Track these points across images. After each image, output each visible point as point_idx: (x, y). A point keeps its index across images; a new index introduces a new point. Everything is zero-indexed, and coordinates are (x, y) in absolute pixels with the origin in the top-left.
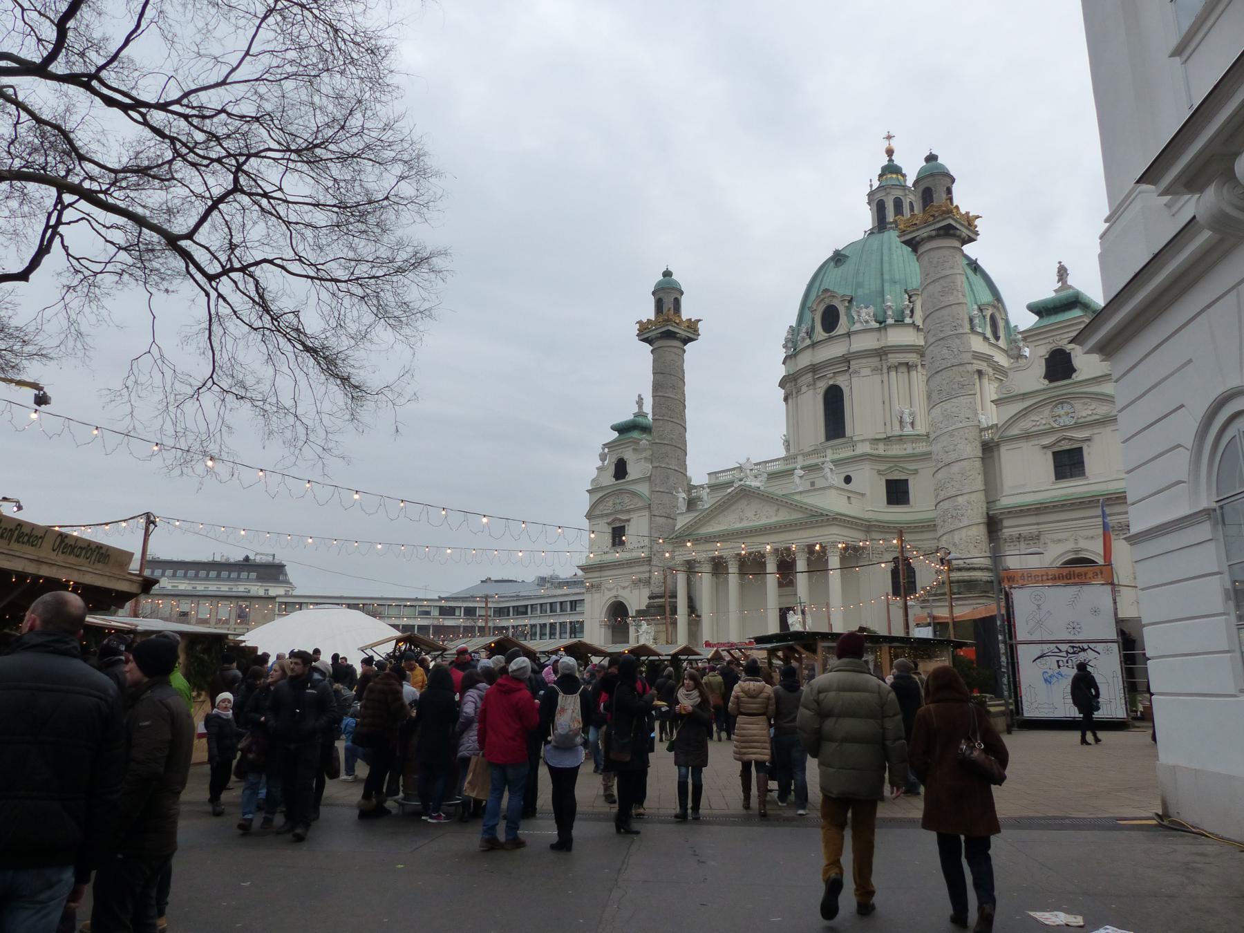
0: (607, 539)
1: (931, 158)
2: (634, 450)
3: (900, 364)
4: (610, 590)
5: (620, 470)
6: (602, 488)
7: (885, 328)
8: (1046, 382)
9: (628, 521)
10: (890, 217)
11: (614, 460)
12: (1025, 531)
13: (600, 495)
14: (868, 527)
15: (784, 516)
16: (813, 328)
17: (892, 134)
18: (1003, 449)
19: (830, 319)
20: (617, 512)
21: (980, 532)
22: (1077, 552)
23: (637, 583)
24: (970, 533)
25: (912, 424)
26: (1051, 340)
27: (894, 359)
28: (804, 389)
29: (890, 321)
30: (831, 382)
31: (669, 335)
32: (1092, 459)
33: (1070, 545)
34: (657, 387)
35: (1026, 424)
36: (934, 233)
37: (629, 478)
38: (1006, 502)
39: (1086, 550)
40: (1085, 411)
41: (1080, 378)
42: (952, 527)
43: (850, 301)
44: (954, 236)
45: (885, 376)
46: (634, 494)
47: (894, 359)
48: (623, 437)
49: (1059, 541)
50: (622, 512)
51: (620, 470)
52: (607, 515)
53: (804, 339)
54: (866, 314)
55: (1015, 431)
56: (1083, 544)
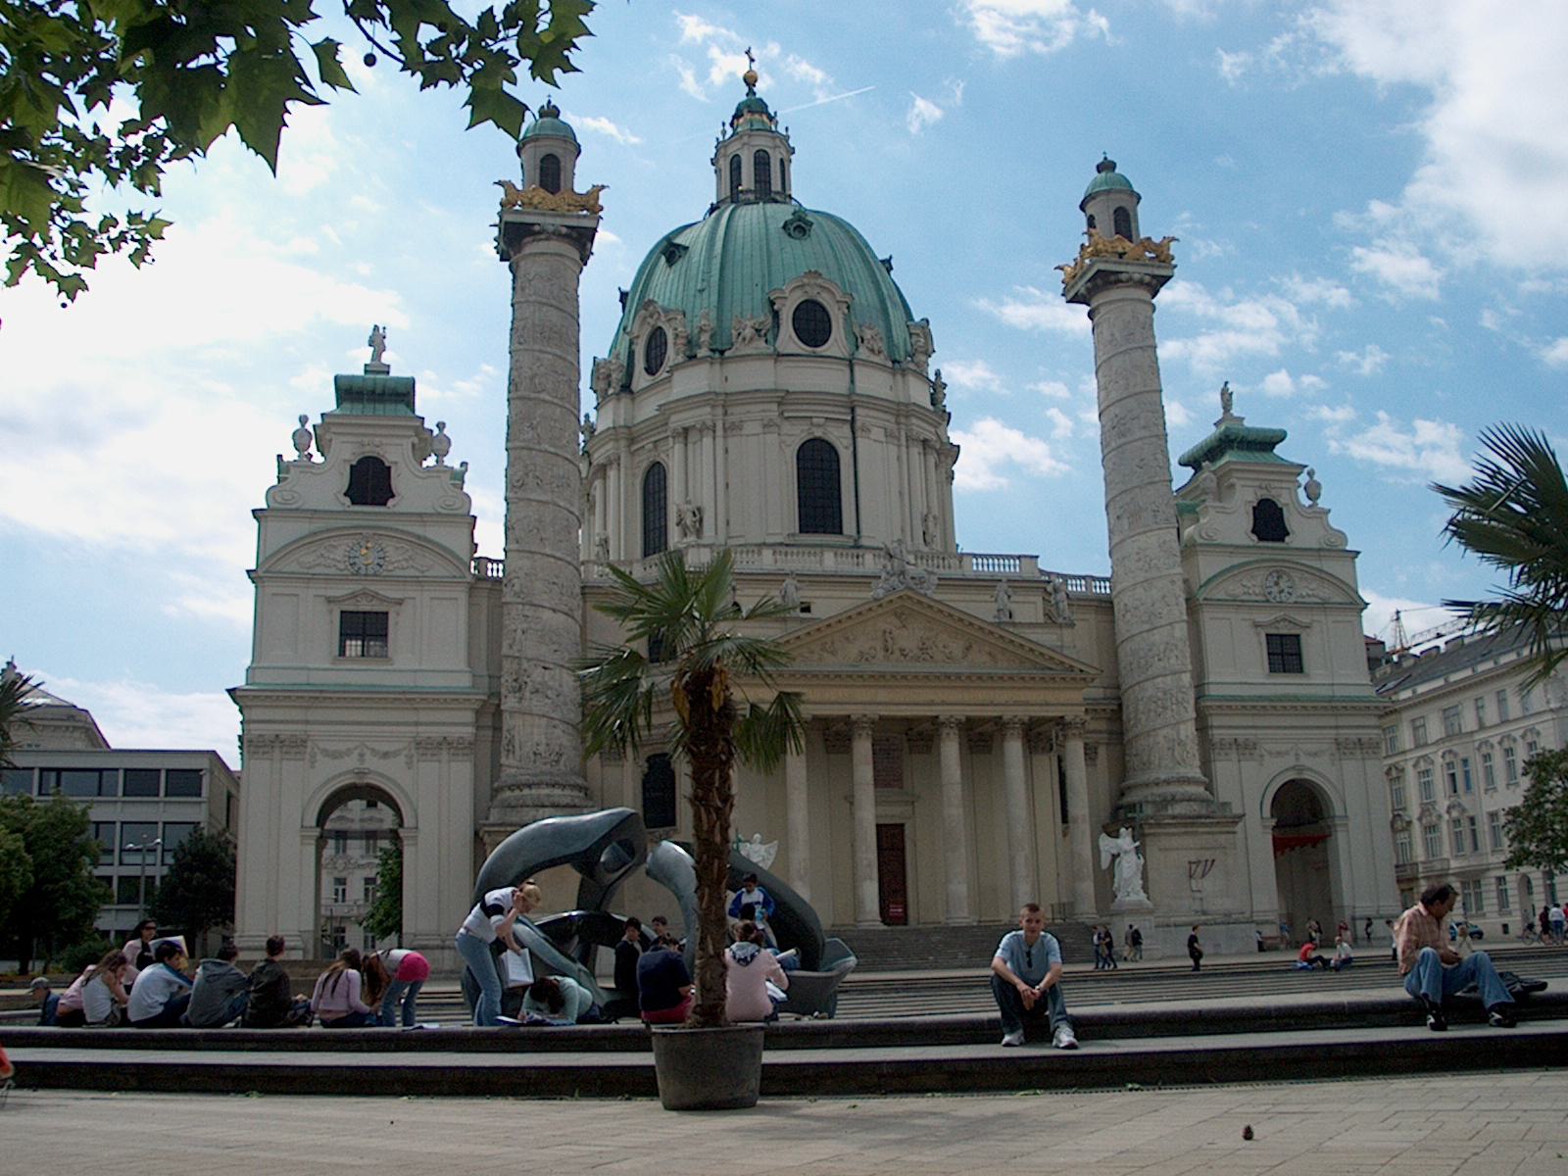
0: (329, 626)
1: (1106, 166)
2: (413, 445)
4: (336, 755)
5: (370, 482)
7: (904, 372)
8: (1255, 537)
9: (400, 602)
10: (776, 186)
13: (302, 528)
16: (777, 324)
19: (812, 324)
22: (1300, 769)
23: (427, 748)
28: (753, 427)
30: (818, 433)
33: (1290, 761)
35: (1233, 588)
36: (1147, 279)
38: (1213, 691)
39: (1310, 769)
41: (1295, 545)
45: (904, 449)
46: (423, 543)
51: (370, 482)
56: (1305, 761)
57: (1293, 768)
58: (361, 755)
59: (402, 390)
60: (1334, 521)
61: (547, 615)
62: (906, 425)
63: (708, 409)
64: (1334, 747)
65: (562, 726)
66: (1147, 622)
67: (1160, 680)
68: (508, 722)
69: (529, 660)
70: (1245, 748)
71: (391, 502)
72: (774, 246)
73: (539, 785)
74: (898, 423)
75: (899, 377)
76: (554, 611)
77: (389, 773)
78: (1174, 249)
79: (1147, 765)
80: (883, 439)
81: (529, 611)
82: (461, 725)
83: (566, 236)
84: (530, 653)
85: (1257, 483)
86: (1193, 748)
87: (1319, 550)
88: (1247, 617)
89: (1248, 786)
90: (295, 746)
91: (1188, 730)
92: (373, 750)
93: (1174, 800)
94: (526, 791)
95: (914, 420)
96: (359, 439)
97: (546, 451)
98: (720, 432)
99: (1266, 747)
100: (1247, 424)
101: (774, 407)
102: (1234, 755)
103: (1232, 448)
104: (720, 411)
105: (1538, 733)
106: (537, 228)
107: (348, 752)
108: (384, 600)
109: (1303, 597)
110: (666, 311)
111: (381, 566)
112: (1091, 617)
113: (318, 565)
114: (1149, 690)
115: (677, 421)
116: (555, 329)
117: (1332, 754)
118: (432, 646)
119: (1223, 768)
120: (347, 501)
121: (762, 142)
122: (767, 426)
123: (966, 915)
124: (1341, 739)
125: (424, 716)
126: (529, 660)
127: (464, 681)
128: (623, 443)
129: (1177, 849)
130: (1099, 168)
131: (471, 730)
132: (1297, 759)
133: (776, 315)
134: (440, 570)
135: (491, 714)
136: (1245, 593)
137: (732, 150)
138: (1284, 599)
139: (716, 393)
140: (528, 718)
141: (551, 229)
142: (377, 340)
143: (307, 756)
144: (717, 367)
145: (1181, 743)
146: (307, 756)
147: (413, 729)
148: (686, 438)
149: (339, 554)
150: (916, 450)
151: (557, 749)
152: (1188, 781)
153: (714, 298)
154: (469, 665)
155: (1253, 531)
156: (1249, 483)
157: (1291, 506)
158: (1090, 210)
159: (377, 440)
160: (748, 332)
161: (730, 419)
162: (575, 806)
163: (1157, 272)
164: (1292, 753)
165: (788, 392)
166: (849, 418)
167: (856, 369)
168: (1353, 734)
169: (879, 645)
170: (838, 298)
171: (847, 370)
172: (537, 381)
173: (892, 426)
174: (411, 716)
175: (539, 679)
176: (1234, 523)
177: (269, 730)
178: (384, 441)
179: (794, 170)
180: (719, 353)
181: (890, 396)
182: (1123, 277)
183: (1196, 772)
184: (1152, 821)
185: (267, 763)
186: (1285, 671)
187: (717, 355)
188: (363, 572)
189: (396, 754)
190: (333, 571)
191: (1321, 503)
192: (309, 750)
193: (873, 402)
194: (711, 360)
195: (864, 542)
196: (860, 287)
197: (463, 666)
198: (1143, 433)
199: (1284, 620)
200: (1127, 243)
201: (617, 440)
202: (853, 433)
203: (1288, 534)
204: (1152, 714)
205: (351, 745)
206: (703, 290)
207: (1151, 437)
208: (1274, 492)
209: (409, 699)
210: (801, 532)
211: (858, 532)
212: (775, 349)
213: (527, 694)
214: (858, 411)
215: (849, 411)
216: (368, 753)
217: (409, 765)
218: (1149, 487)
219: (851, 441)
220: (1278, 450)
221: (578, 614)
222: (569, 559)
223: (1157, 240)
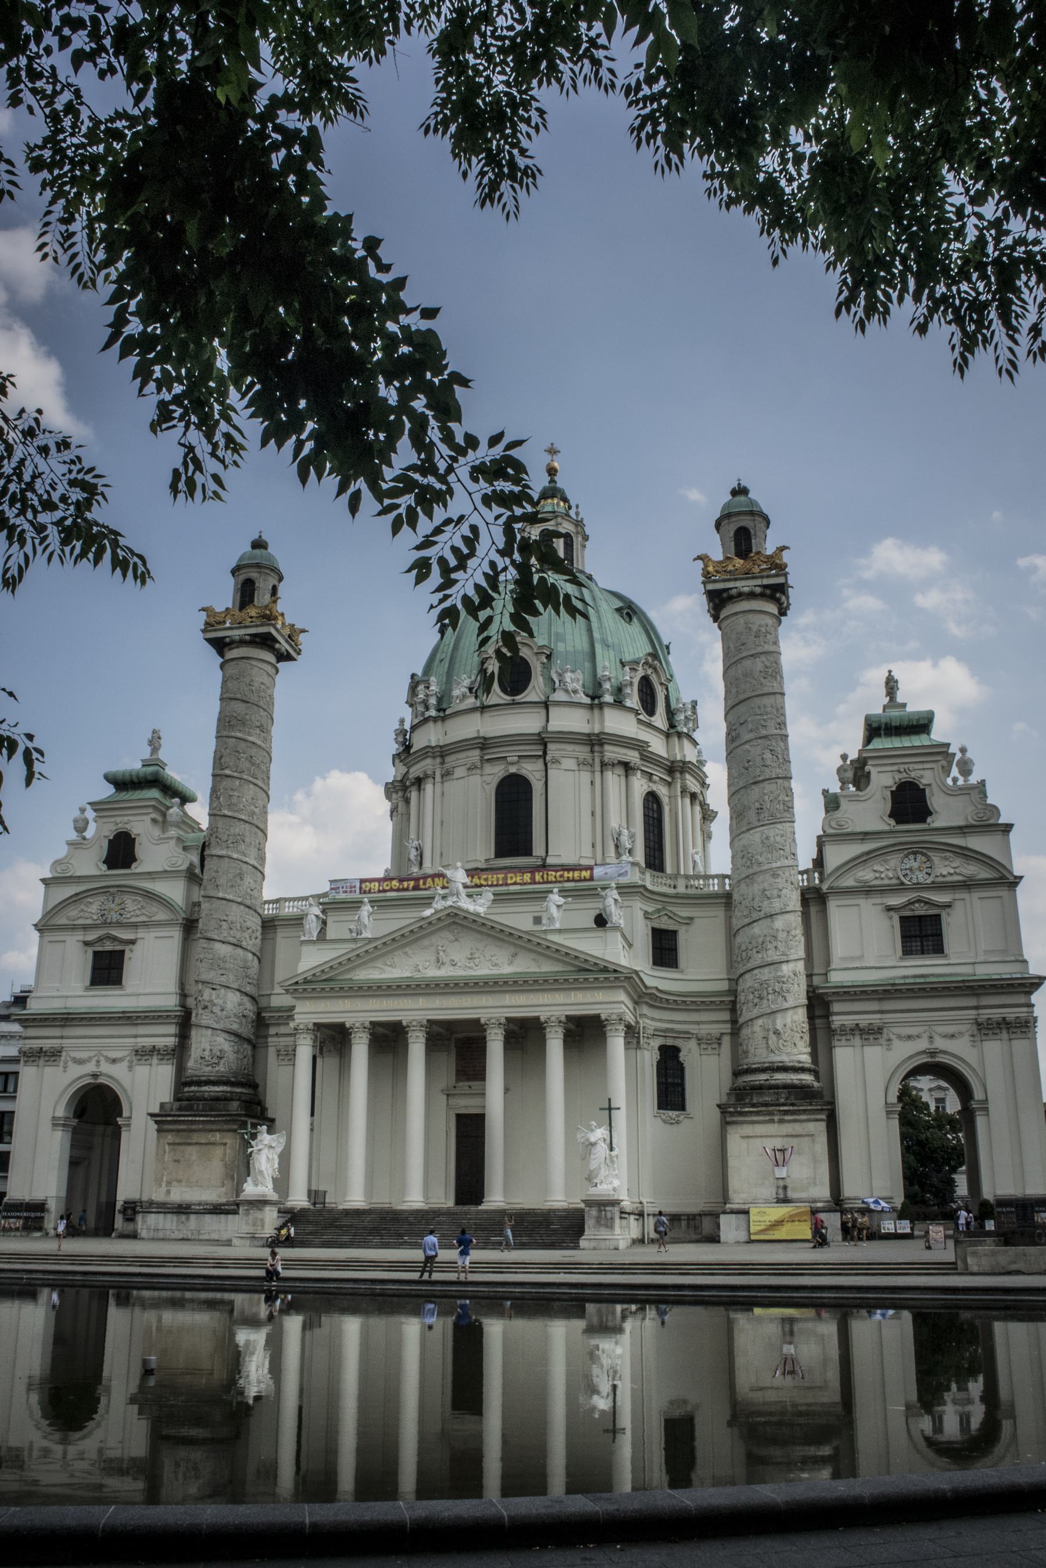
1: (740, 491)
2: (154, 821)
3: (620, 763)
4: (80, 1062)
5: (121, 851)
7: (601, 706)
8: (892, 822)
9: (133, 942)
11: (110, 830)
12: (864, 1020)
14: (643, 996)
15: (524, 965)
17: (558, 446)
18: (832, 905)
20: (106, 924)
21: (800, 1016)
22: (933, 1053)
24: (796, 1018)
25: (630, 851)
26: (902, 768)
27: (612, 753)
28: (460, 772)
29: (608, 698)
30: (513, 770)
31: (266, 641)
33: (923, 1044)
34: (227, 724)
35: (865, 875)
36: (758, 590)
37: (136, 868)
38: (837, 978)
39: (945, 1052)
40: (945, 868)
42: (774, 1007)
43: (549, 657)
44: (778, 601)
47: (612, 753)
48: (124, 795)
49: (909, 1037)
51: (121, 851)
52: (85, 928)
53: (464, 696)
54: (575, 680)
55: (848, 882)
56: (940, 1044)
57: (924, 1052)
58: (98, 1061)
59: (150, 778)
61: (218, 946)
62: (601, 752)
63: (429, 761)
64: (975, 1027)
65: (226, 1036)
66: (746, 917)
67: (756, 971)
68: (194, 1033)
69: (203, 983)
70: (870, 1034)
71: (134, 865)
73: (200, 1083)
74: (592, 752)
75: (596, 711)
76: (223, 942)
79: (746, 1052)
80: (576, 768)
82: (165, 1036)
84: (204, 977)
85: (895, 768)
87: (960, 828)
88: (878, 901)
91: (795, 1019)
92: (107, 1058)
94: (193, 1088)
95: (607, 747)
96: (113, 819)
97: (225, 816)
99: (896, 1030)
100: (909, 709)
101: (477, 752)
102: (857, 1041)
103: (879, 736)
104: (438, 760)
106: (228, 640)
109: (944, 876)
111: (121, 915)
112: (720, 913)
113: (81, 917)
114: (748, 982)
115: (416, 771)
116: (239, 718)
117: (973, 1036)
118: (153, 973)
119: (845, 1057)
120: (104, 867)
123: (562, 1198)
124: (982, 1019)
128: (400, 794)
129: (761, 1137)
130: (735, 493)
132: (931, 1042)
134: (162, 915)
136: (876, 878)
138: (921, 880)
139: (433, 748)
142: (155, 742)
144: (439, 723)
145: (777, 1033)
146: (62, 1064)
147: (132, 1040)
148: (419, 786)
149: (94, 908)
151: (218, 1054)
152: (785, 1069)
153: (447, 666)
155: (890, 816)
156: (889, 768)
157: (934, 786)
162: (226, 1099)
163: (766, 582)
164: (925, 1036)
165: (485, 739)
166: (541, 753)
167: (551, 709)
168: (996, 1014)
169: (433, 959)
170: (535, 651)
171: (543, 712)
172: (223, 760)
180: (443, 713)
181: (585, 729)
182: (734, 592)
183: (805, 1059)
184: (732, 1110)
186: (923, 953)
187: (441, 714)
188: (109, 921)
189: (121, 1060)
192: (63, 1058)
194: (435, 719)
195: (550, 861)
196: (569, 637)
198: (751, 736)
199: (919, 901)
200: (739, 562)
201: (397, 792)
202: (546, 765)
203: (931, 814)
204: (750, 1004)
206: (441, 661)
207: (756, 739)
208: (913, 774)
210: (496, 857)
211: (547, 852)
212: (482, 703)
214: (550, 746)
215: (541, 747)
216: (102, 1059)
217: (130, 1068)
218: (753, 787)
219: (544, 774)
221: (253, 942)
222: (240, 900)
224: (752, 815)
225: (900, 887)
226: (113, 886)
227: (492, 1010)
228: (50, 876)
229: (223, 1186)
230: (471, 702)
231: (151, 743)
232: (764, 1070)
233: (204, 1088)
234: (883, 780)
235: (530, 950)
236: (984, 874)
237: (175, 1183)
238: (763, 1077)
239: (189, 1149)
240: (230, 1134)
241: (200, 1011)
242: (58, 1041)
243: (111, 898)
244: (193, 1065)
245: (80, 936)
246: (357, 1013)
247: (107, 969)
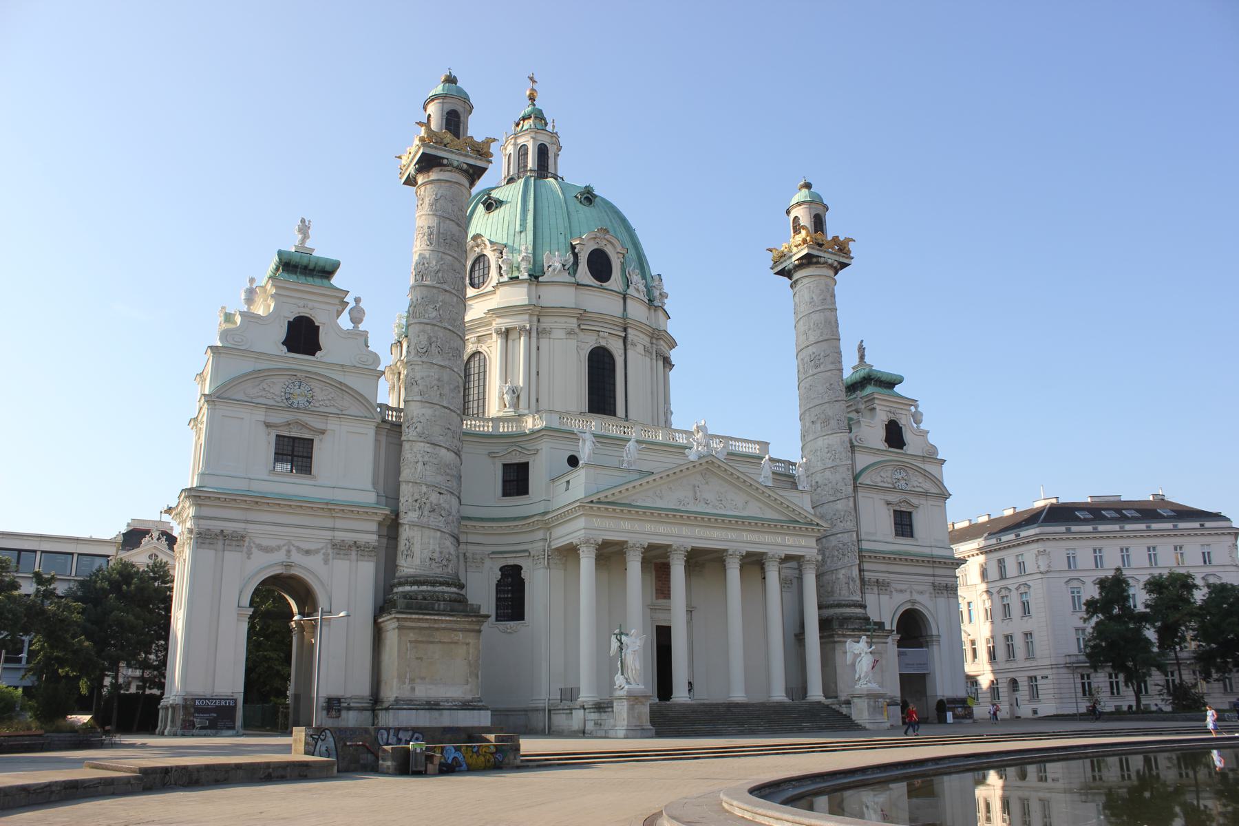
0: (267, 447)
4: (268, 550)
5: (303, 336)
6: (260, 355)
9: (323, 432)
10: (551, 169)
12: (881, 576)
13: (247, 366)
16: (576, 262)
18: (861, 494)
19: (600, 266)
22: (914, 602)
23: (341, 548)
30: (603, 343)
32: (920, 522)
33: (907, 597)
36: (836, 264)
38: (865, 545)
46: (342, 388)
49: (901, 591)
50: (312, 413)
51: (303, 336)
56: (916, 597)
58: (289, 551)
59: (328, 268)
60: (931, 439)
61: (444, 451)
63: (527, 317)
65: (452, 539)
68: (405, 533)
70: (882, 586)
71: (318, 354)
72: (571, 208)
73: (433, 584)
77: (312, 569)
78: (851, 245)
79: (832, 592)
81: (428, 448)
83: (466, 172)
86: (858, 582)
89: (885, 609)
90: (233, 540)
91: (856, 571)
92: (298, 548)
93: (850, 618)
94: (424, 588)
98: (534, 334)
101: (575, 320)
102: (875, 588)
104: (535, 319)
105: (1029, 587)
106: (445, 162)
107: (279, 548)
108: (311, 429)
110: (491, 242)
119: (871, 599)
120: (285, 348)
121: (544, 139)
122: (570, 333)
125: (339, 524)
126: (428, 486)
127: (371, 498)
131: (375, 537)
133: (576, 256)
134: (355, 410)
135: (391, 528)
137: (521, 141)
140: (427, 532)
141: (455, 164)
142: (304, 229)
143: (245, 549)
146: (245, 549)
147: (329, 534)
150: (661, 363)
154: (375, 484)
158: (793, 214)
159: (310, 304)
160: (558, 265)
161: (543, 325)
167: (629, 301)
173: (648, 345)
174: (329, 523)
175: (435, 502)
176: (874, 433)
177: (216, 526)
178: (316, 305)
179: (559, 160)
182: (822, 260)
185: (213, 552)
189: (317, 551)
190: (271, 402)
191: (923, 426)
193: (639, 326)
197: (370, 487)
198: (832, 367)
205: (281, 543)
209: (330, 508)
213: (426, 513)
214: (630, 331)
217: (326, 562)
220: (897, 389)
223: (842, 239)
224: (833, 423)
225: (894, 489)
226: (301, 371)
227: (738, 542)
228: (220, 344)
229: (467, 683)
230: (566, 277)
231: (300, 230)
232: (849, 606)
233: (437, 589)
234: (882, 417)
235: (758, 500)
236: (934, 490)
237: (418, 681)
238: (848, 610)
239: (431, 646)
240: (472, 634)
241: (426, 513)
242: (242, 525)
243: (297, 384)
244: (408, 566)
245: (260, 415)
246: (639, 533)
247: (295, 452)
